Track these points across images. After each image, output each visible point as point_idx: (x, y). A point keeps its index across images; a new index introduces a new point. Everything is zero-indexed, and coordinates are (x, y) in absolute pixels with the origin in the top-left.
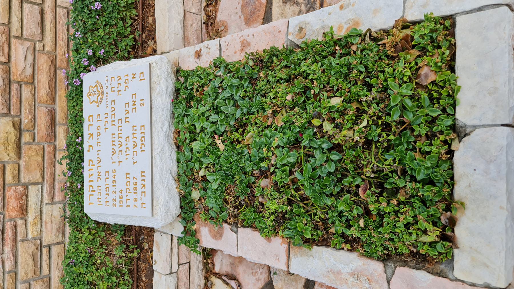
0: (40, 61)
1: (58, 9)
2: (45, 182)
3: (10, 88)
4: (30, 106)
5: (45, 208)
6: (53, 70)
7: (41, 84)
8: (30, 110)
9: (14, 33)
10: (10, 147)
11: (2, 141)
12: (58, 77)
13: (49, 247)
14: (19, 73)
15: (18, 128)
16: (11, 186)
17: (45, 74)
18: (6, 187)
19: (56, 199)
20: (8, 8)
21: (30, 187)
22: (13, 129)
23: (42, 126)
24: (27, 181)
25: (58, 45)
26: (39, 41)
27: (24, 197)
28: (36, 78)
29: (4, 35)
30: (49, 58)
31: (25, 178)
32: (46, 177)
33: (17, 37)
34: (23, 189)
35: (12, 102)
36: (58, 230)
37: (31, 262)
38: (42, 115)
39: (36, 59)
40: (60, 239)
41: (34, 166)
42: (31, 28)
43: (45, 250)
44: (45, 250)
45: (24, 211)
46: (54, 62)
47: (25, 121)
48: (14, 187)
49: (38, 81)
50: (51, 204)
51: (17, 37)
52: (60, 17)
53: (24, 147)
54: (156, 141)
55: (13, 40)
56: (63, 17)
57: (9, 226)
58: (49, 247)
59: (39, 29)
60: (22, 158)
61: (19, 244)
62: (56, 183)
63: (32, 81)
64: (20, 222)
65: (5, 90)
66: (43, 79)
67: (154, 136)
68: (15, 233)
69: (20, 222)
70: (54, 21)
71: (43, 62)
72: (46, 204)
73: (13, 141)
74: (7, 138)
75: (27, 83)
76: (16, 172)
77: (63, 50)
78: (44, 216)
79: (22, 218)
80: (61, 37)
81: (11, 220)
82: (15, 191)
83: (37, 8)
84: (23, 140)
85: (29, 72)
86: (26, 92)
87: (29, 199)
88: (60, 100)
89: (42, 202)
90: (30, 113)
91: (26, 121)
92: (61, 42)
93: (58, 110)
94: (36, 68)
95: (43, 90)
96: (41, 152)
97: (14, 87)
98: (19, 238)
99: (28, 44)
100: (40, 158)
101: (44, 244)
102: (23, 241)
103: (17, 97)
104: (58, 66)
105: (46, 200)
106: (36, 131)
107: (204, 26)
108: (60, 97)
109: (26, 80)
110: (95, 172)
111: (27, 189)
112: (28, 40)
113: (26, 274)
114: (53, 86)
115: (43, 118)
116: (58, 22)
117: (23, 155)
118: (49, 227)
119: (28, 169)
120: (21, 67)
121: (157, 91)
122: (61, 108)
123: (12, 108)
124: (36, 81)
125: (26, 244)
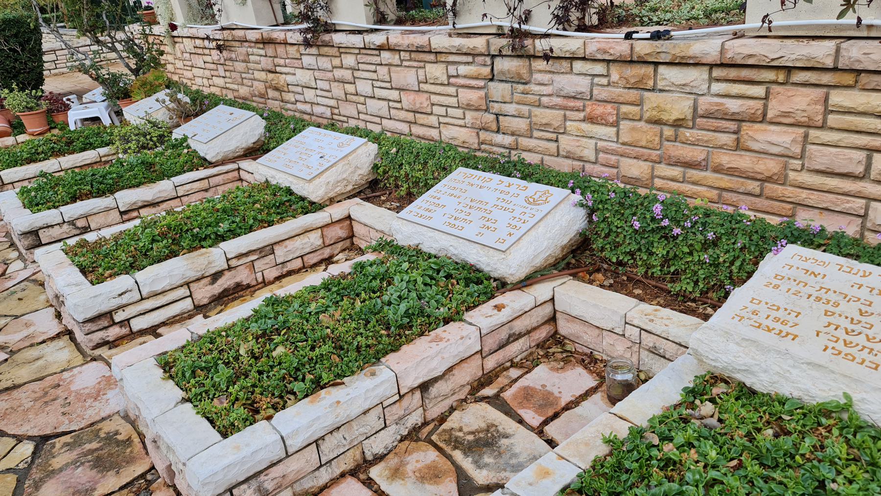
0: (772, 162)
1: (864, 201)
2: (619, 146)
3: (733, 120)
4: (706, 141)
5: (593, 141)
6: (759, 177)
7: (737, 158)
8: (702, 140)
9: (813, 133)
10: (654, 113)
11: (661, 105)
12: (750, 181)
13: (557, 141)
14: (750, 133)
15: (678, 124)
16: (618, 110)
17: (750, 166)
18: (616, 105)
19: (601, 155)
20: (853, 128)
21: (615, 129)
22: (674, 118)
23: (681, 152)
24: (621, 127)
25: (801, 190)
26: (803, 165)
27: (603, 121)
28: (748, 153)
29: (807, 119)
30: (775, 174)
31: (624, 125)
32: (625, 147)
33: (806, 136)
34: (611, 121)
35: (714, 121)
36: (568, 152)
37: (544, 121)
38: (695, 154)
39: (777, 158)
40: (561, 153)
41: (637, 136)
42: (821, 157)
43: (554, 136)
44: (554, 136)
45: (591, 119)
46: (769, 179)
47: (688, 133)
48: (615, 112)
49: (741, 155)
50: (596, 150)
51: (806, 136)
52: (848, 202)
53: (657, 128)
54: (444, 236)
55: (802, 131)
56: (848, 205)
57: (579, 104)
58: (557, 141)
59: (822, 168)
60: (647, 125)
61: (562, 112)
62: (617, 157)
63: (739, 146)
64: (581, 115)
65: (726, 114)
66: (744, 162)
67: (449, 236)
68: (572, 109)
69: (581, 115)
70: (840, 191)
71: (771, 166)
72: (596, 144)
73: (662, 117)
74: (665, 111)
75: (738, 140)
76: (631, 116)
77: (791, 195)
78: (585, 140)
79: (585, 117)
80: (812, 197)
81: (584, 106)
82: (609, 114)
83: (860, 169)
84: (665, 128)
85: (755, 146)
86: (726, 139)
87: (603, 127)
88: (717, 179)
89: (601, 139)
90: (698, 140)
91: (688, 135)
92: (804, 196)
93: (703, 174)
94: (762, 156)
95: (726, 159)
96: (651, 146)
97: (733, 126)
98: (568, 113)
99: (797, 149)
100: (644, 143)
101: (560, 136)
102: (565, 115)
103: (718, 127)
104: (766, 184)
105: (601, 144)
106: (676, 144)
107: (589, 351)
108: (721, 179)
109: (742, 140)
110: (475, 181)
111: (612, 125)
112: (803, 150)
113: (536, 116)
114: (736, 174)
115: (691, 154)
116: (839, 197)
117: (649, 126)
118: (573, 143)
119: (633, 129)
120: (760, 137)
121: (481, 252)
122: (705, 177)
123: (705, 120)
124: (743, 153)
125: (561, 118)
